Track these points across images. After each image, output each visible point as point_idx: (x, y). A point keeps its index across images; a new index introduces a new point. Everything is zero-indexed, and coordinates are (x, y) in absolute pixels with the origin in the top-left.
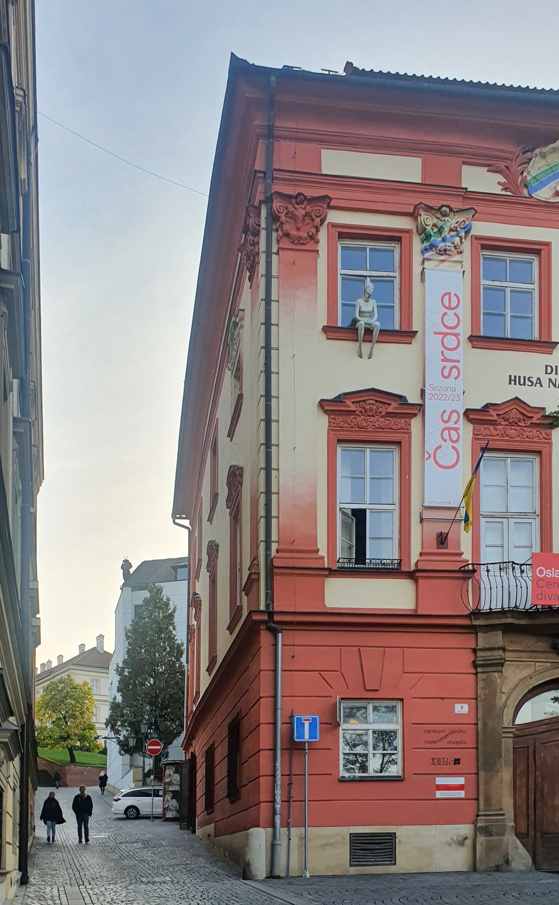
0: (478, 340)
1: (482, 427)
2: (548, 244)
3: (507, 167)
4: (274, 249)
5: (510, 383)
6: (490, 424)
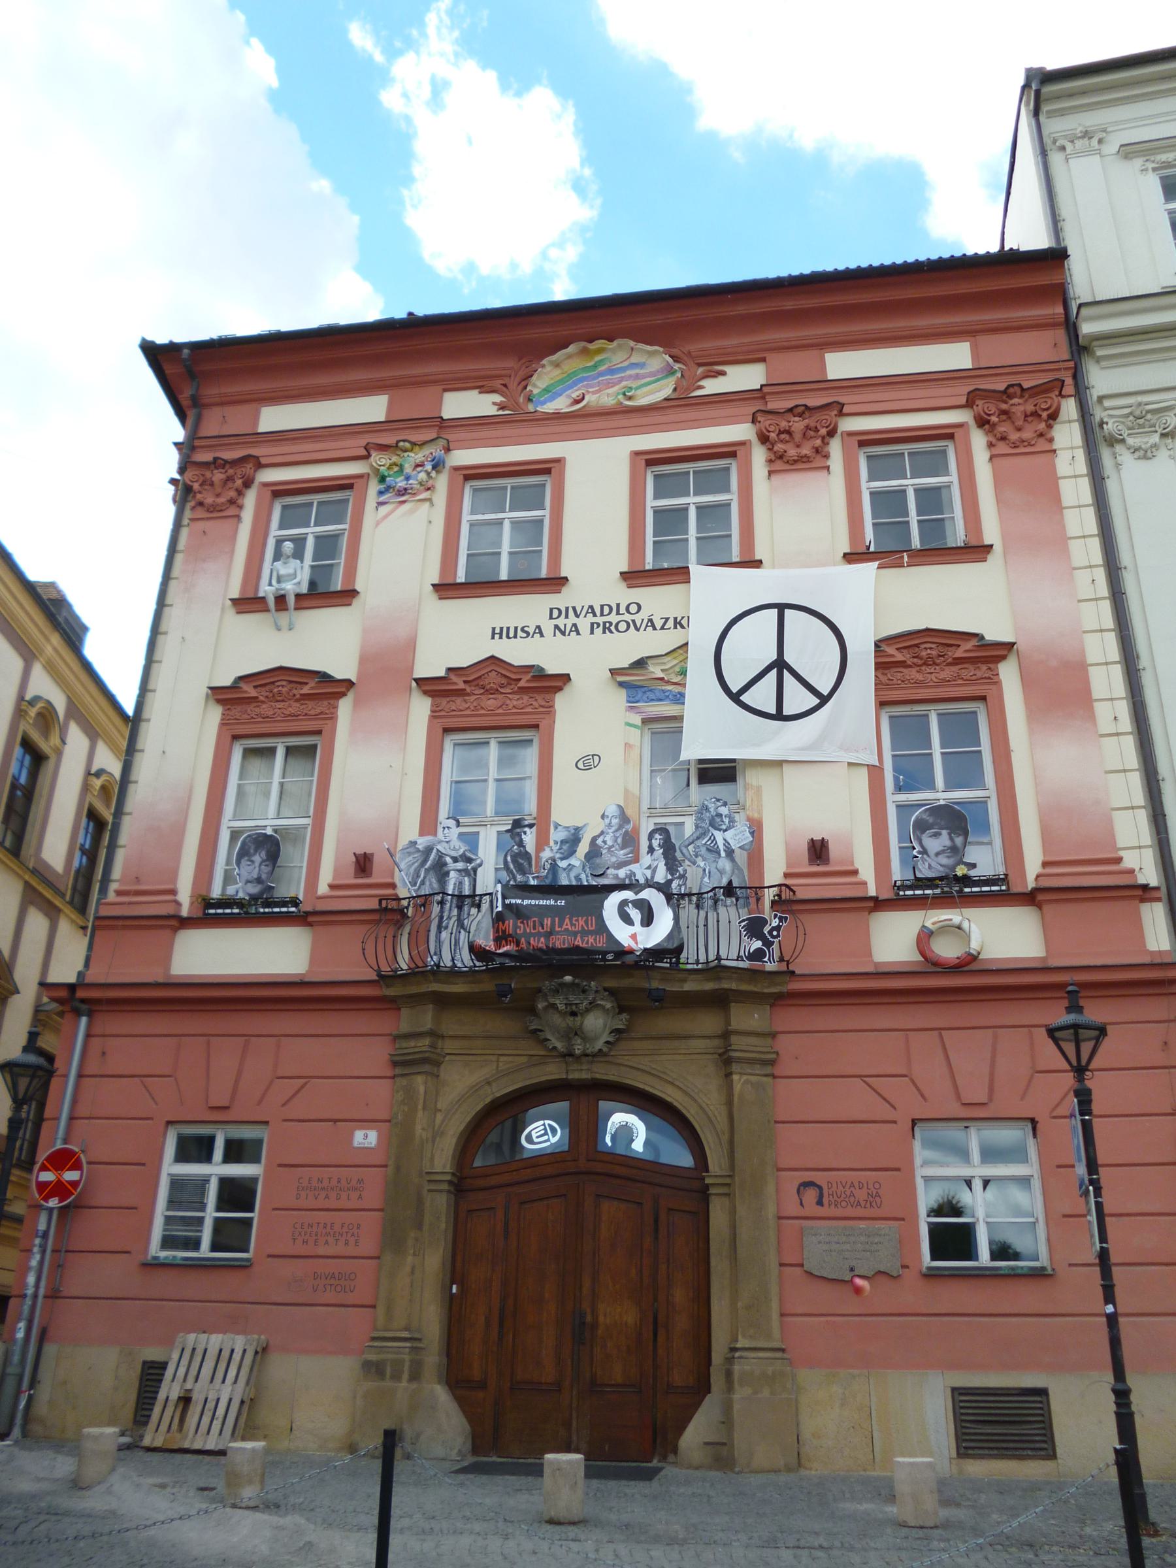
0: (446, 589)
1: (444, 701)
2: (559, 461)
3: (505, 385)
4: (185, 521)
5: (493, 638)
6: (458, 696)
